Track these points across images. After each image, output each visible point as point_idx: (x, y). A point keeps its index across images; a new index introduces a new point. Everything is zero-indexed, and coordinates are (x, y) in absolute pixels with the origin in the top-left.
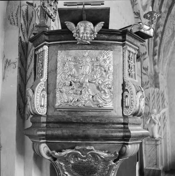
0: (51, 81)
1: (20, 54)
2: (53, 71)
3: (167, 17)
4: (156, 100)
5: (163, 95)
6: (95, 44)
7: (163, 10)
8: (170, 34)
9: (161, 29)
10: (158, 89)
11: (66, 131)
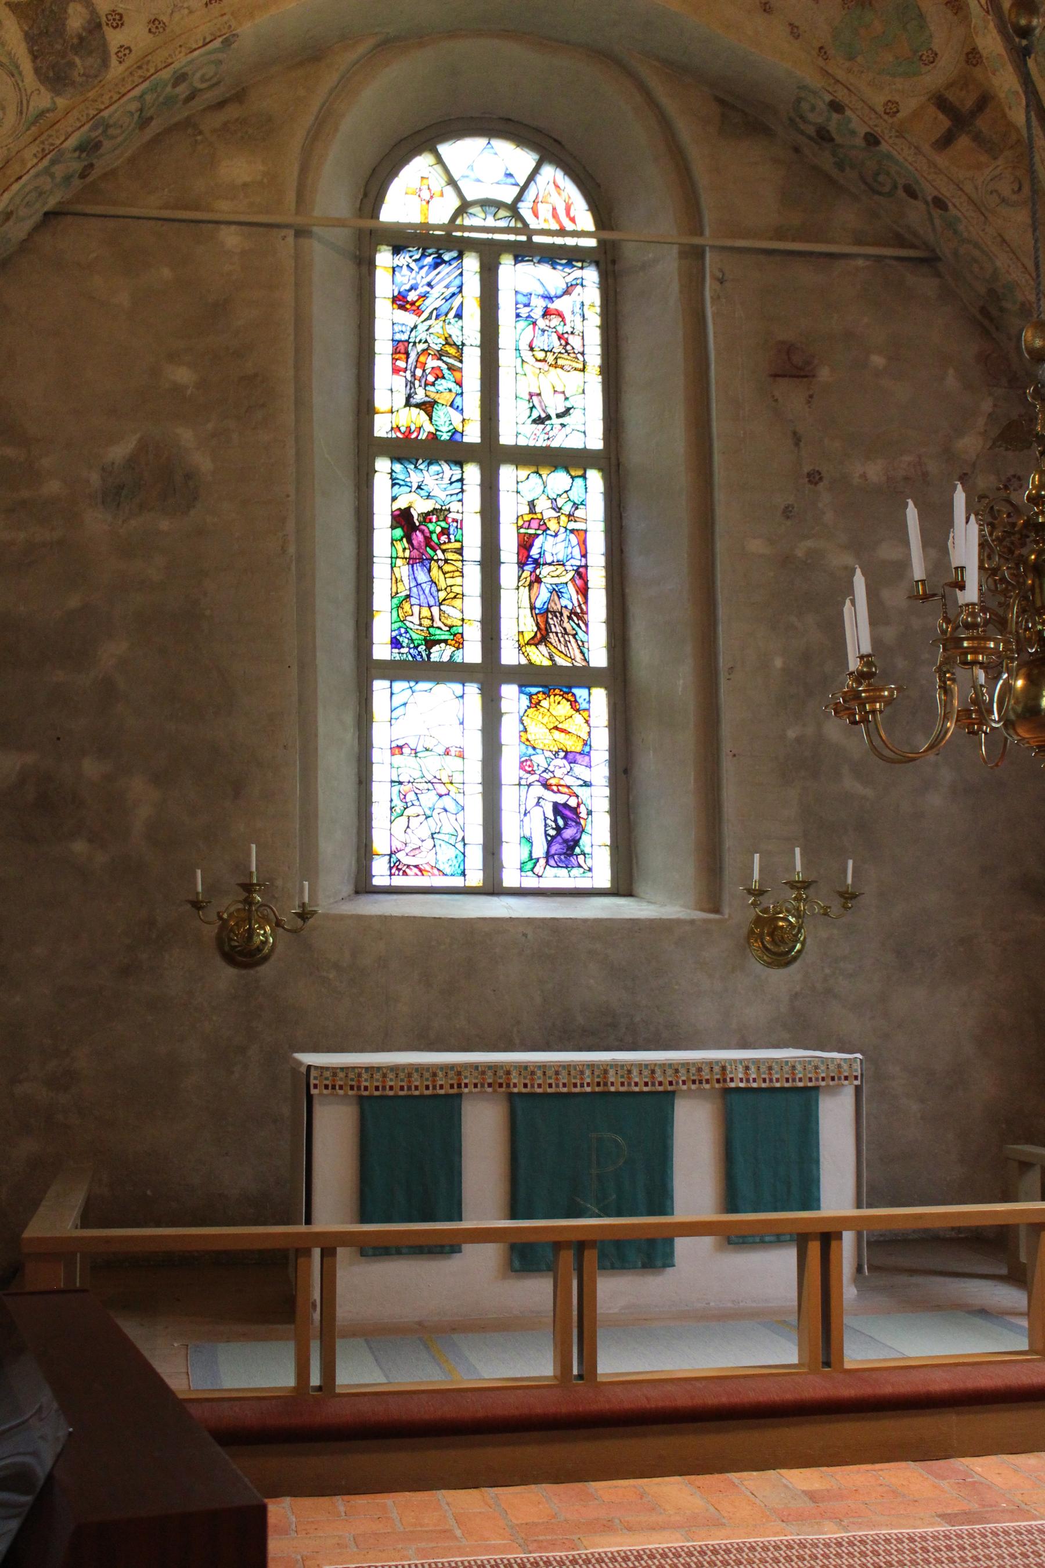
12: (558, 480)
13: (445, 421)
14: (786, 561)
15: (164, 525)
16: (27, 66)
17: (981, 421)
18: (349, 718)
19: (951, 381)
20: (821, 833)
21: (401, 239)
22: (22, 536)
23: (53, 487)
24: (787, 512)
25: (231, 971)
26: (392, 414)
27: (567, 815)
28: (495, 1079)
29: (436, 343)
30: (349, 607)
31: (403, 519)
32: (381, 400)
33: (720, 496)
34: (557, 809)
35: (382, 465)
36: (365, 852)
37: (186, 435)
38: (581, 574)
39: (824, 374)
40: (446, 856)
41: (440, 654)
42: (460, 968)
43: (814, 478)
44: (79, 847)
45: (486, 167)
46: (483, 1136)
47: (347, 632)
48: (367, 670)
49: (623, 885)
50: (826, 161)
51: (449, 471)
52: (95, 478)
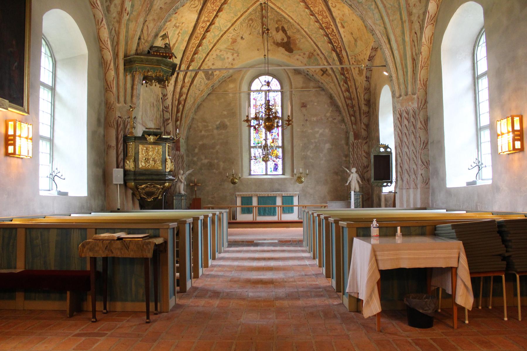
2: (137, 153)
3: (190, 86)
5: (182, 157)
6: (154, 143)
7: (186, 80)
9: (184, 96)
11: (144, 177)
14: (302, 132)
15: (224, 131)
18: (248, 154)
19: (326, 106)
20: (306, 166)
21: (254, 91)
23: (210, 128)
24: (303, 125)
27: (276, 165)
28: (257, 195)
34: (275, 164)
36: (250, 170)
37: (226, 120)
39: (308, 106)
43: (307, 120)
44: (215, 171)
47: (247, 143)
48: (250, 147)
49: (283, 174)
52: (215, 126)
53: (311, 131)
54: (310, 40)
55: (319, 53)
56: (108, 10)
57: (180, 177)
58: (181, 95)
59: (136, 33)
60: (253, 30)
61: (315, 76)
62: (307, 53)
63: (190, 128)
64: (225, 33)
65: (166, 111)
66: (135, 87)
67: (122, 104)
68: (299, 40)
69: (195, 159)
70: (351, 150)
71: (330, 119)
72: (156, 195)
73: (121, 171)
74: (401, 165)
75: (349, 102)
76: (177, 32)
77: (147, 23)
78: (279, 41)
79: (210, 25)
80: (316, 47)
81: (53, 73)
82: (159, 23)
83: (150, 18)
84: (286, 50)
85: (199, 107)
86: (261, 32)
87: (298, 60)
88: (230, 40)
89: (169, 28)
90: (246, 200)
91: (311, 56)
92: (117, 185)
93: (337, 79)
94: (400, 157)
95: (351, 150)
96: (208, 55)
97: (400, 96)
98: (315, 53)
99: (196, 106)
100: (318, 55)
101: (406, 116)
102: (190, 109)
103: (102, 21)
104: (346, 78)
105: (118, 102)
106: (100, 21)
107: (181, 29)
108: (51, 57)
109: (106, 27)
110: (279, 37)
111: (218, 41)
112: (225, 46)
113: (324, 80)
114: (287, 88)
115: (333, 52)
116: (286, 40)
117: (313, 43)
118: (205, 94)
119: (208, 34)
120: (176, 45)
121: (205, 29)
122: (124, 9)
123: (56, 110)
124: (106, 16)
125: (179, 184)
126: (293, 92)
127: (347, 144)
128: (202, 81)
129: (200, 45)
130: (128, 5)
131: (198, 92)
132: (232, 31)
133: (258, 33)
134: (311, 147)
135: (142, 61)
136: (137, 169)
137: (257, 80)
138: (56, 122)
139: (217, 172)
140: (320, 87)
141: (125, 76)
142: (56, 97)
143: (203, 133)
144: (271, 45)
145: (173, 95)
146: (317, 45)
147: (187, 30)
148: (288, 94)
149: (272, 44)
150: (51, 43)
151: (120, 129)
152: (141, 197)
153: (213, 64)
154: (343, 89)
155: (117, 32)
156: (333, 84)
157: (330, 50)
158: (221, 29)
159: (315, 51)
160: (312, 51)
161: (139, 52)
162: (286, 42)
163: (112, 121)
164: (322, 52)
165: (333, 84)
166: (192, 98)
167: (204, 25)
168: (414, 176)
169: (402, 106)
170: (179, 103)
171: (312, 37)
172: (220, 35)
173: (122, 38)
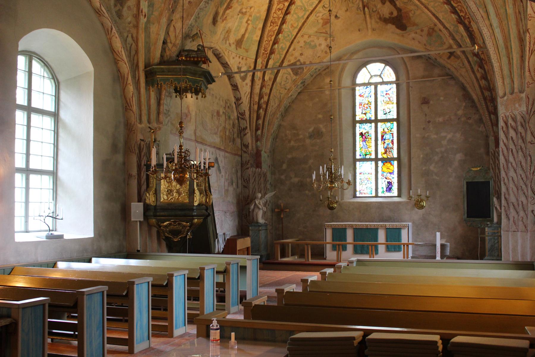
0: (158, 189)
1: (138, 171)
4: (257, 183)
5: (265, 175)
7: (267, 78)
8: (277, 105)
9: (266, 98)
10: (260, 170)
11: (166, 213)
12: (388, 124)
13: (368, 117)
14: (424, 138)
15: (318, 141)
16: (291, 73)
17: (463, 108)
18: (351, 169)
19: (457, 101)
21: (360, 85)
22: (297, 145)
23: (301, 136)
24: (424, 129)
25: (329, 211)
26: (359, 116)
27: (390, 183)
28: (351, 226)
29: (367, 102)
30: (352, 150)
31: (361, 134)
32: (357, 113)
33: (412, 127)
34: (388, 182)
35: (358, 125)
36: (355, 191)
37: (321, 126)
38: (392, 141)
39: (431, 102)
40: (368, 191)
41: (368, 157)
42: (366, 209)
43: (429, 122)
44: (307, 192)
45: (376, 68)
46: (350, 234)
47: (351, 154)
49: (399, 196)
50: (431, 61)
51: (369, 125)
52: (307, 134)
53: (436, 136)
54: (426, 11)
55: (441, 27)
56: (119, 15)
57: (257, 202)
58: (261, 97)
59: (159, 35)
60: (350, 5)
61: (438, 60)
62: (426, 29)
63: (275, 138)
64: (311, 13)
65: (242, 119)
66: (162, 102)
67: (145, 124)
68: (413, 12)
69: (283, 177)
70: (491, 162)
71: (463, 119)
72: (183, 234)
73: (141, 204)
74: (507, 196)
75: (487, 93)
76: (245, 20)
77: (173, 23)
78: (387, 16)
79: (290, 5)
80: (436, 21)
81: (55, 96)
82: (188, 21)
83: (177, 16)
84: (398, 27)
85: (287, 110)
86: (361, 6)
87: (414, 39)
88: (321, 21)
89: (232, 17)
90: (339, 234)
91: (431, 32)
92: (137, 221)
93: (469, 62)
94: (505, 184)
95: (491, 162)
96: (292, 43)
97: (505, 94)
98: (436, 28)
99: (282, 109)
100: (440, 30)
101: (513, 124)
102: (274, 114)
103: (112, 29)
104: (481, 60)
105: (141, 123)
106: (110, 29)
107: (250, 16)
108: (53, 78)
109: (117, 35)
110: (386, 10)
111: (303, 24)
112: (315, 29)
113: (452, 65)
114: (403, 78)
115: (459, 25)
116: (395, 13)
117: (431, 15)
118: (294, 93)
119: (288, 17)
120: (246, 36)
121: (284, 11)
122: (140, 11)
123: (60, 139)
124: (116, 22)
125: (256, 210)
126: (411, 84)
127: (488, 153)
128: (289, 77)
129: (279, 32)
130: (144, 6)
131: (284, 92)
132: (321, 9)
133: (358, 8)
134: (436, 158)
135: (163, 72)
136: (158, 203)
137: (364, 69)
138: (60, 152)
139: (310, 194)
140: (448, 75)
141: (147, 90)
142: (60, 124)
143: (292, 143)
144: (377, 22)
145: (251, 97)
146: (437, 18)
147: (258, 15)
148: (404, 86)
149: (378, 21)
150: (50, 64)
151: (143, 154)
152: (165, 236)
153: (301, 54)
154: (479, 75)
155: (135, 39)
156: (464, 70)
157: (456, 23)
158: (305, 8)
159: (435, 25)
160: (432, 25)
161: (165, 59)
162: (397, 17)
163: (133, 146)
164: (444, 27)
165: (464, 70)
166: (276, 99)
167: (281, 6)
168: (522, 213)
169: (507, 109)
170: (259, 107)
171: (430, 7)
172: (306, 17)
173: (141, 44)
